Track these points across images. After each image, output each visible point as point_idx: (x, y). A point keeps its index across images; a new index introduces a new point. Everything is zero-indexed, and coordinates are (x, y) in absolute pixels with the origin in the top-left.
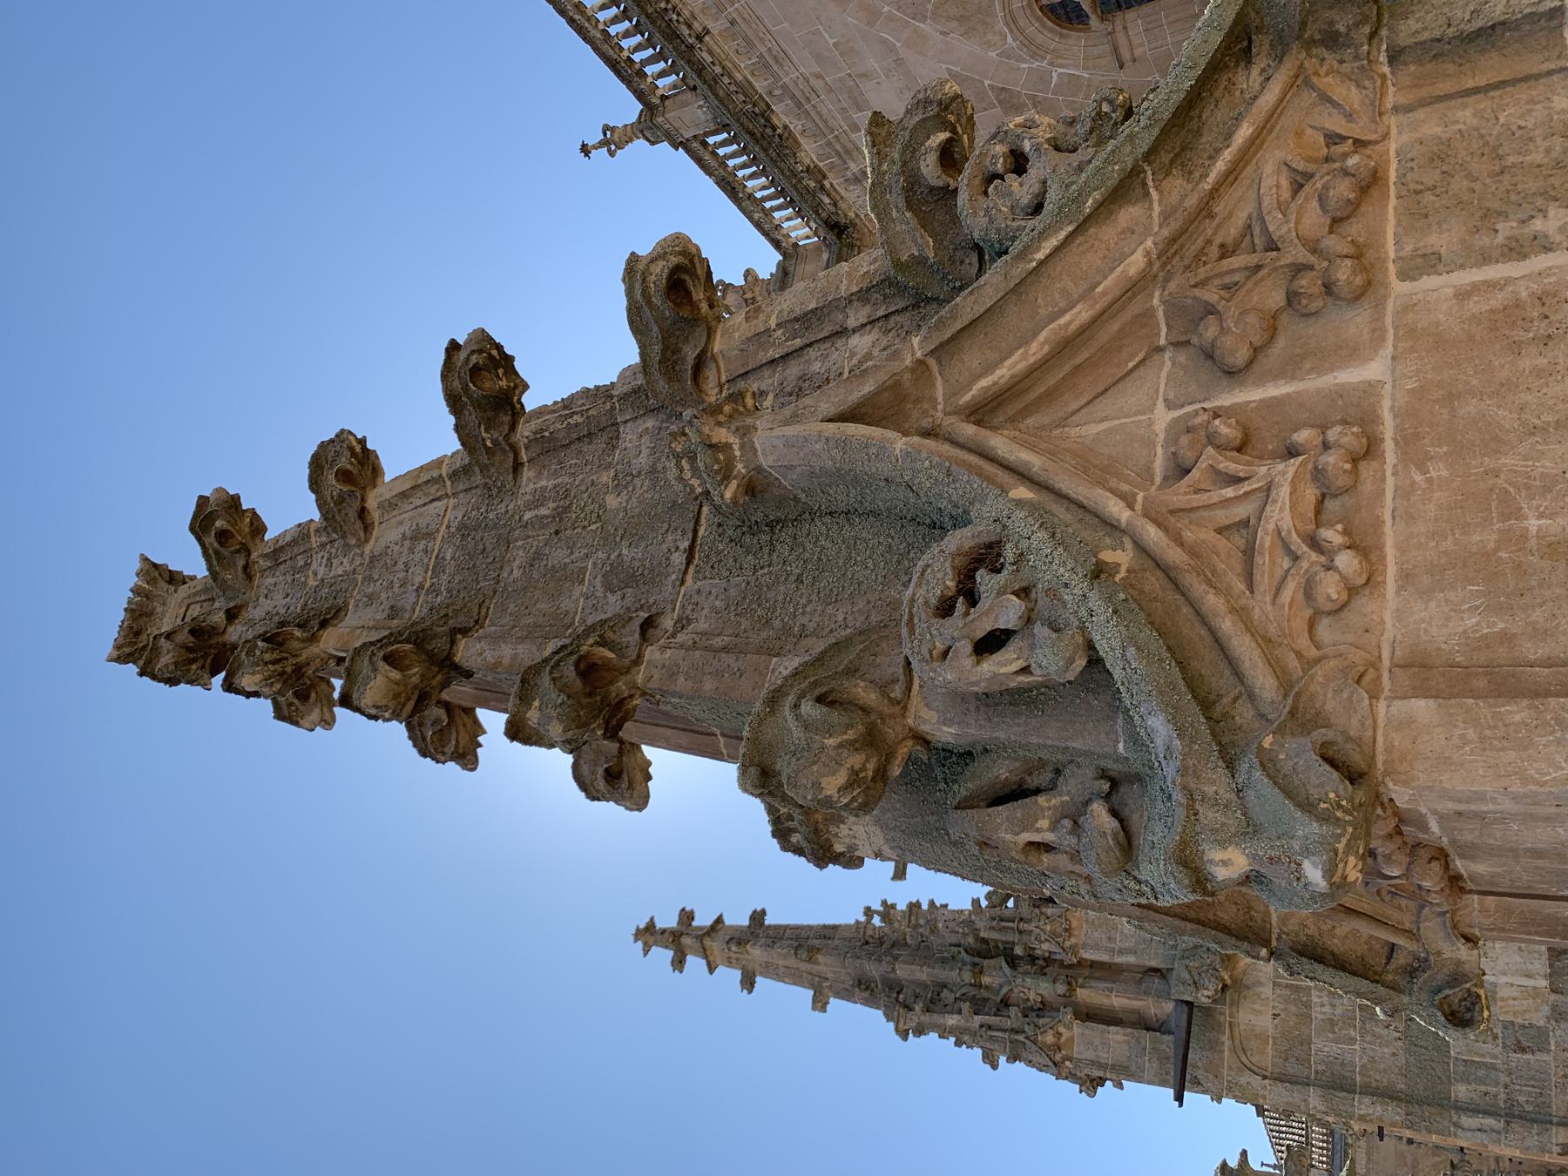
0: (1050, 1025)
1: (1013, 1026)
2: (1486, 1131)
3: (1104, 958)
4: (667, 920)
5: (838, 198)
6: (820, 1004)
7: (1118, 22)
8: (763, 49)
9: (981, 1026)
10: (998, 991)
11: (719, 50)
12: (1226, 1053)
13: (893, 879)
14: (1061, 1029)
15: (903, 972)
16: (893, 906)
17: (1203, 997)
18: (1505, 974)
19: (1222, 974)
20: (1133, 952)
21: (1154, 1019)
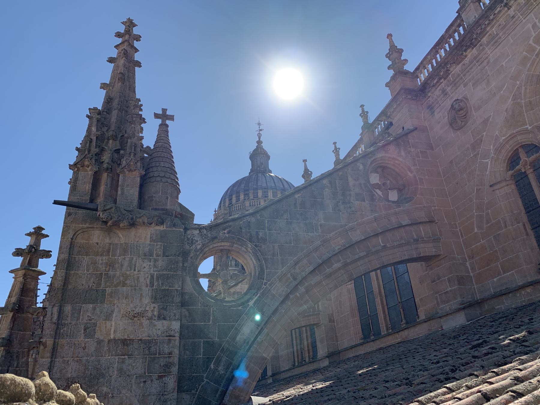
0: (91, 163)
1: (91, 151)
2: (52, 315)
3: (120, 183)
4: (136, 31)
5: (436, 87)
6: (103, 86)
7: (510, 182)
8: (500, 35)
9: (91, 139)
11: (500, 16)
12: (81, 225)
14: (90, 167)
15: (115, 113)
18: (115, 324)
20: (122, 193)
21: (96, 202)
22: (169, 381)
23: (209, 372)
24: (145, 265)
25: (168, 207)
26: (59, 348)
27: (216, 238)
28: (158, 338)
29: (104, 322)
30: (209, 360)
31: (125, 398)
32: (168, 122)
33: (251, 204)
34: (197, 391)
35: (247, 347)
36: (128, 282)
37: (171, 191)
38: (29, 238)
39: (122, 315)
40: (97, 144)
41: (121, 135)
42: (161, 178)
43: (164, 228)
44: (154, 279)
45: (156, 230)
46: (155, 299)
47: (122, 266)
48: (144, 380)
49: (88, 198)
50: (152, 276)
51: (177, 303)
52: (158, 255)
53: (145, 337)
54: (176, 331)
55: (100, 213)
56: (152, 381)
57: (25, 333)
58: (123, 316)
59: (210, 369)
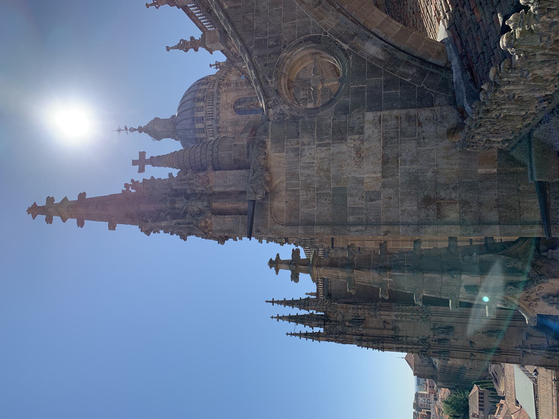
0: (202, 219)
2: (358, 231)
9: (176, 224)
10: (182, 209)
13: (138, 172)
14: (207, 220)
16: (137, 182)
17: (258, 197)
18: (367, 173)
19: (266, 188)
21: (243, 211)
22: (424, 115)
23: (414, 82)
24: (308, 154)
25: (245, 143)
26: (389, 221)
27: (277, 91)
28: (382, 131)
29: (365, 185)
30: (403, 83)
31: (438, 154)
32: (147, 157)
33: (211, 135)
34: (433, 92)
35: (391, 47)
36: (325, 167)
37: (227, 142)
38: (280, 271)
39: (358, 168)
40: (181, 218)
41: (168, 197)
42: (214, 153)
43: (268, 141)
44: (322, 144)
45: (271, 148)
46: (343, 139)
47: (309, 175)
48: (422, 139)
49: (240, 217)
50: (319, 145)
51: (347, 118)
52: (298, 143)
53: (380, 144)
54: (374, 115)
55: (258, 197)
56: (423, 132)
57: (372, 260)
58: (359, 167)
59: (411, 81)
